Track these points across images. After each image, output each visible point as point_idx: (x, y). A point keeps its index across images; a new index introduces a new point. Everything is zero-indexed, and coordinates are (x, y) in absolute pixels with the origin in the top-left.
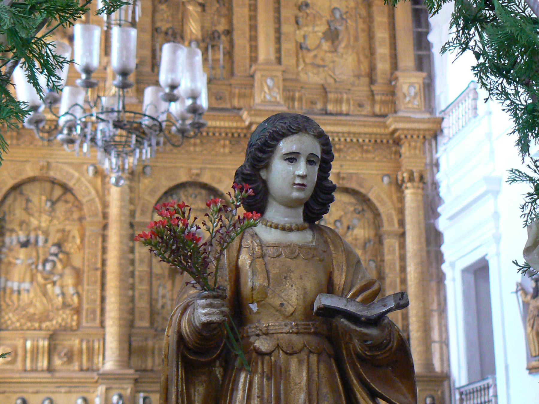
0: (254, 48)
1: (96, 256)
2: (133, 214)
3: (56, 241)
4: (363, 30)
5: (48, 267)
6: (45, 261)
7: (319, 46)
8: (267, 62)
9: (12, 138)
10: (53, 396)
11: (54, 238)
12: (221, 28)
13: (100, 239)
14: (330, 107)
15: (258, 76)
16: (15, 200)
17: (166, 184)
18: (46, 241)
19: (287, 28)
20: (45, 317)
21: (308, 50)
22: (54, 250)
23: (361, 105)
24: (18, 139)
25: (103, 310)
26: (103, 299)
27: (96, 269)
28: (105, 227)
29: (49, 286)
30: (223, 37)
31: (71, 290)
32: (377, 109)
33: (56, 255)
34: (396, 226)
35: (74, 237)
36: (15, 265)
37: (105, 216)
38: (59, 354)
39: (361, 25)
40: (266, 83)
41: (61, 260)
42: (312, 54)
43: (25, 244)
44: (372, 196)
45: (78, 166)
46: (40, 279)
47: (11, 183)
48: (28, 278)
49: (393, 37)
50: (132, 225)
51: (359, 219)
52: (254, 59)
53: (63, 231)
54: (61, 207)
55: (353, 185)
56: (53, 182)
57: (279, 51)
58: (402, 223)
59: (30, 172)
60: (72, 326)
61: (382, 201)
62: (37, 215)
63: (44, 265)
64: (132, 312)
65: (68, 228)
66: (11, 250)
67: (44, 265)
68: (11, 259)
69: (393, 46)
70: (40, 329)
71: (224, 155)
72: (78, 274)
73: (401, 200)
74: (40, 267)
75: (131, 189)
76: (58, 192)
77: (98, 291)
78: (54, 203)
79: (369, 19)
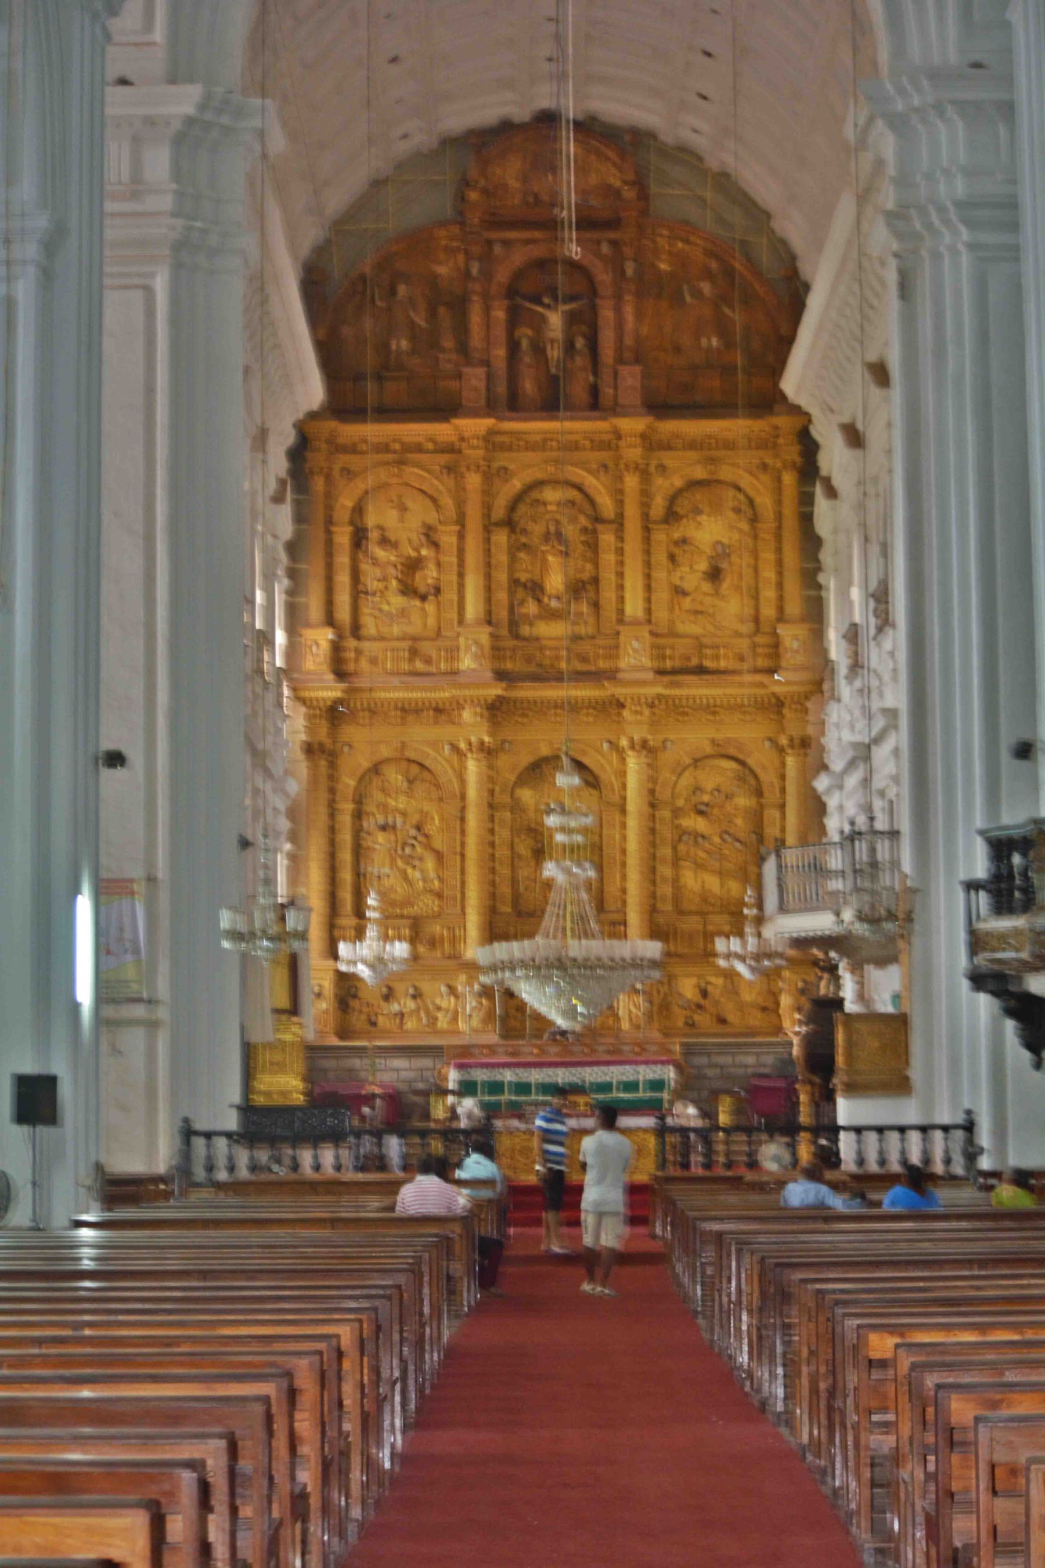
0: (621, 599)
1: (455, 840)
2: (492, 792)
3: (414, 822)
4: (748, 566)
5: (408, 850)
6: (404, 845)
7: (697, 588)
8: (636, 623)
9: (364, 718)
10: (417, 984)
11: (415, 818)
12: (586, 576)
13: (458, 822)
14: (708, 664)
15: (622, 638)
16: (371, 780)
17: (526, 759)
18: (404, 823)
19: (660, 575)
20: (408, 902)
21: (685, 594)
22: (413, 832)
23: (742, 659)
24: (371, 718)
25: (463, 894)
26: (463, 883)
27: (455, 854)
28: (463, 809)
29: (410, 871)
30: (588, 587)
31: (432, 874)
32: (761, 662)
33: (415, 838)
34: (778, 795)
35: (433, 819)
36: (374, 849)
37: (463, 797)
38: (421, 943)
39: (752, 561)
40: (631, 645)
41: (420, 842)
42: (688, 600)
43: (384, 828)
44: (751, 761)
45: (435, 745)
46: (400, 863)
47: (366, 764)
48: (387, 861)
49: (780, 574)
50: (491, 806)
51: (738, 787)
52: (621, 612)
53: (421, 812)
54: (420, 788)
55: (732, 751)
56: (409, 761)
57: (648, 600)
58: (783, 790)
59: (385, 752)
60: (433, 911)
61: (764, 768)
62: (394, 796)
63: (403, 849)
64: (493, 896)
65: (426, 808)
66: (369, 833)
67: (403, 849)
68: (370, 844)
69: (780, 586)
70: (402, 916)
71: (587, 723)
72: (439, 856)
73: (783, 764)
74: (400, 852)
75: (491, 767)
76: (415, 769)
77: (458, 876)
78: (410, 782)
79: (755, 554)
